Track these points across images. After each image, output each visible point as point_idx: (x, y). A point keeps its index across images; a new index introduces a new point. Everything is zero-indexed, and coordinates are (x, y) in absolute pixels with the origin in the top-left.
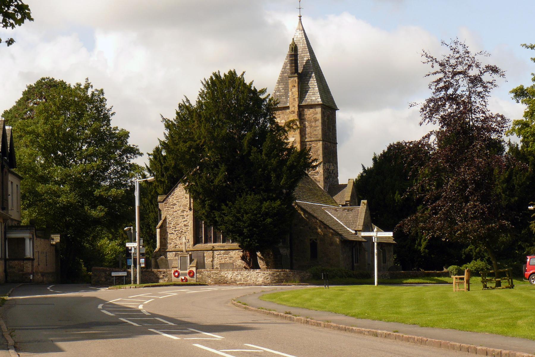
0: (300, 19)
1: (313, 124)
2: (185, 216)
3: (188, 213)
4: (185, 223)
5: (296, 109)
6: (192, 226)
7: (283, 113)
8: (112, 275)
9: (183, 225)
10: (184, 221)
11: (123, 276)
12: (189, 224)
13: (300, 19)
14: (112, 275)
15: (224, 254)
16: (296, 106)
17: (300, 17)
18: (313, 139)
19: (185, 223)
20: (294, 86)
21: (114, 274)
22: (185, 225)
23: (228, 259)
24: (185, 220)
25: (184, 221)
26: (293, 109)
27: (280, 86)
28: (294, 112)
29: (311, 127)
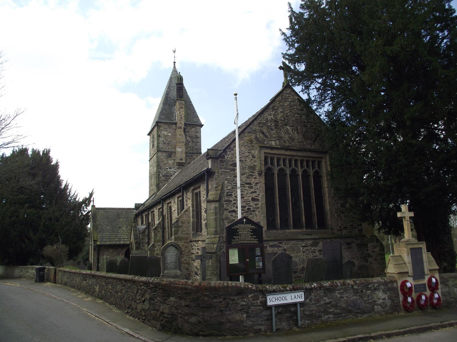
0: (174, 65)
1: (195, 140)
2: (253, 185)
3: (257, 181)
4: (254, 195)
5: (183, 126)
6: (264, 201)
7: (170, 128)
8: (269, 303)
9: (250, 199)
10: (252, 193)
11: (295, 305)
12: (260, 198)
13: (174, 65)
14: (269, 303)
15: (312, 245)
16: (183, 123)
17: (175, 63)
18: (194, 152)
19: (254, 195)
20: (182, 108)
21: (272, 300)
22: (253, 199)
23: (317, 253)
24: (253, 190)
25: (252, 193)
26: (180, 125)
27: (165, 107)
28: (181, 128)
29: (193, 142)
